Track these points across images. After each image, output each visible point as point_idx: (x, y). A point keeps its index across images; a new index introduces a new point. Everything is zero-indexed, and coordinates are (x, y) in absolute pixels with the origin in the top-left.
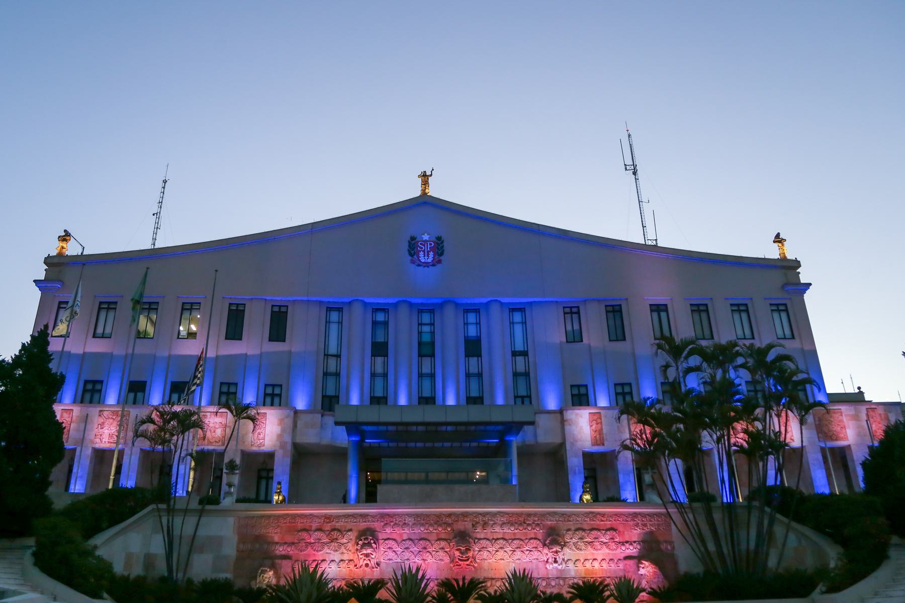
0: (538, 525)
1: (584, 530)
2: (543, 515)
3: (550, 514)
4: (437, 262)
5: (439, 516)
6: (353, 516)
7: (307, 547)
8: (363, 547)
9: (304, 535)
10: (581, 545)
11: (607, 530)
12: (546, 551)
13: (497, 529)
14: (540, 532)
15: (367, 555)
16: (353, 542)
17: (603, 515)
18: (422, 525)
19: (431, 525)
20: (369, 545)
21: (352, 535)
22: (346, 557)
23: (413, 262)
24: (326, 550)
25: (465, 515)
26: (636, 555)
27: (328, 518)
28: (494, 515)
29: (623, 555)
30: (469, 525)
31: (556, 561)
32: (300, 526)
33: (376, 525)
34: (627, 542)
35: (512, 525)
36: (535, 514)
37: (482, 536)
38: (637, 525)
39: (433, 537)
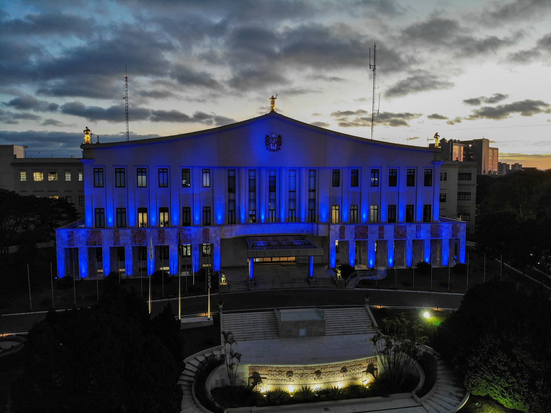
9: (270, 372)
10: (351, 370)
20: (291, 376)
21: (285, 373)
22: (284, 378)
25: (319, 366)
27: (278, 368)
30: (320, 369)
33: (293, 370)
39: (309, 373)
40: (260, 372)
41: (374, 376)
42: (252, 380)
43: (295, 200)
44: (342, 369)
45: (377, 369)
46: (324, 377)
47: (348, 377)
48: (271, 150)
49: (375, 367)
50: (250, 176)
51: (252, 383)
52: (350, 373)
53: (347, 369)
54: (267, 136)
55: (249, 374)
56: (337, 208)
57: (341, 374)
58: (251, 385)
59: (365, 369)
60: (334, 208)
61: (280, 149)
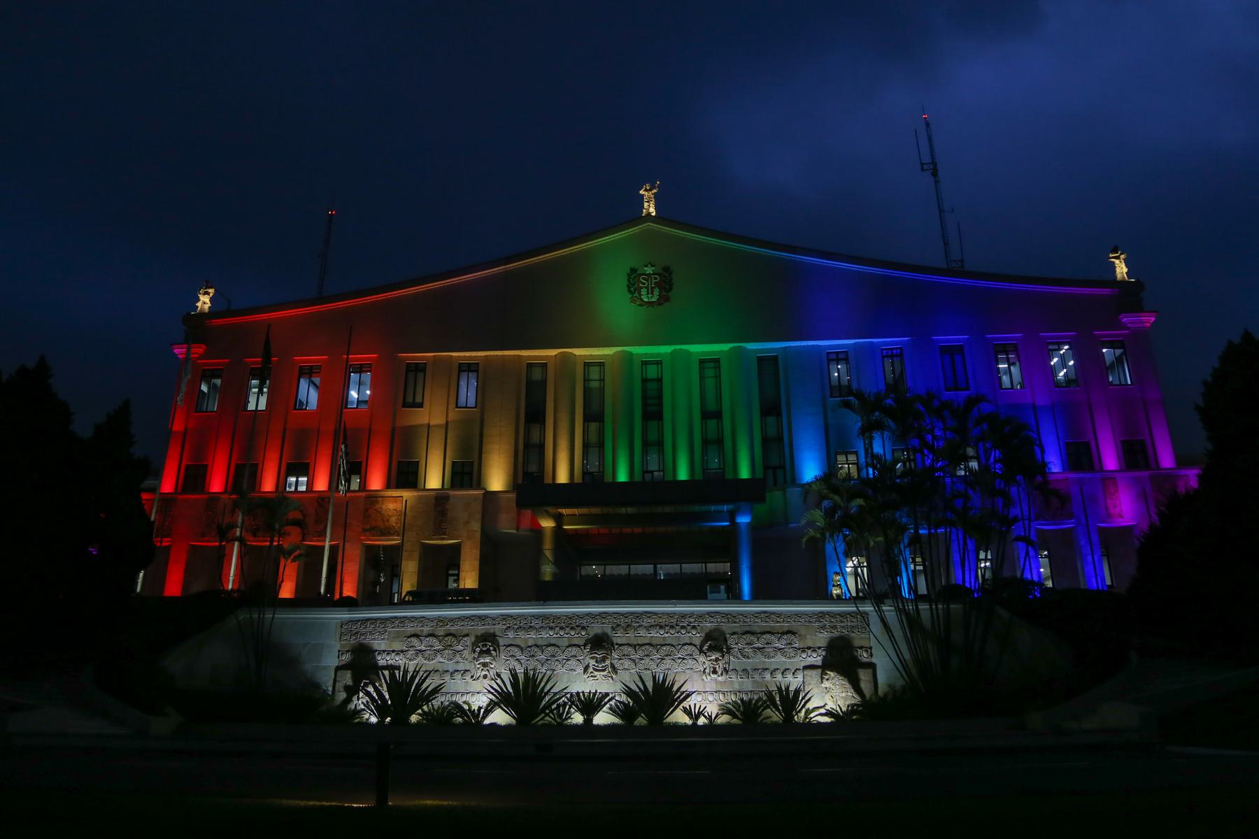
0: (694, 627)
1: (752, 633)
2: (701, 616)
3: (709, 613)
4: (664, 299)
5: (570, 617)
6: (471, 618)
7: (417, 655)
8: (482, 652)
9: (414, 639)
10: (748, 650)
11: (783, 633)
12: (702, 659)
13: (642, 632)
14: (697, 637)
15: (485, 665)
16: (469, 649)
17: (779, 614)
18: (551, 628)
19: (561, 628)
20: (488, 652)
21: (469, 641)
22: (461, 667)
23: (633, 301)
24: (439, 658)
26: (820, 663)
27: (442, 621)
28: (639, 615)
29: (803, 664)
31: (715, 672)
32: (410, 629)
33: (498, 628)
34: (809, 648)
35: (661, 627)
36: (691, 614)
37: (624, 641)
38: (823, 627)
40: (379, 644)
41: (855, 685)
42: (347, 678)
43: (720, 442)
44: (709, 636)
45: (872, 666)
46: (627, 663)
47: (736, 681)
48: (643, 304)
49: (864, 656)
50: (586, 380)
51: (347, 688)
52: (749, 663)
53: (731, 641)
54: (633, 270)
55: (341, 653)
56: (852, 458)
57: (704, 662)
58: (342, 696)
59: (816, 659)
60: (841, 458)
61: (667, 299)
